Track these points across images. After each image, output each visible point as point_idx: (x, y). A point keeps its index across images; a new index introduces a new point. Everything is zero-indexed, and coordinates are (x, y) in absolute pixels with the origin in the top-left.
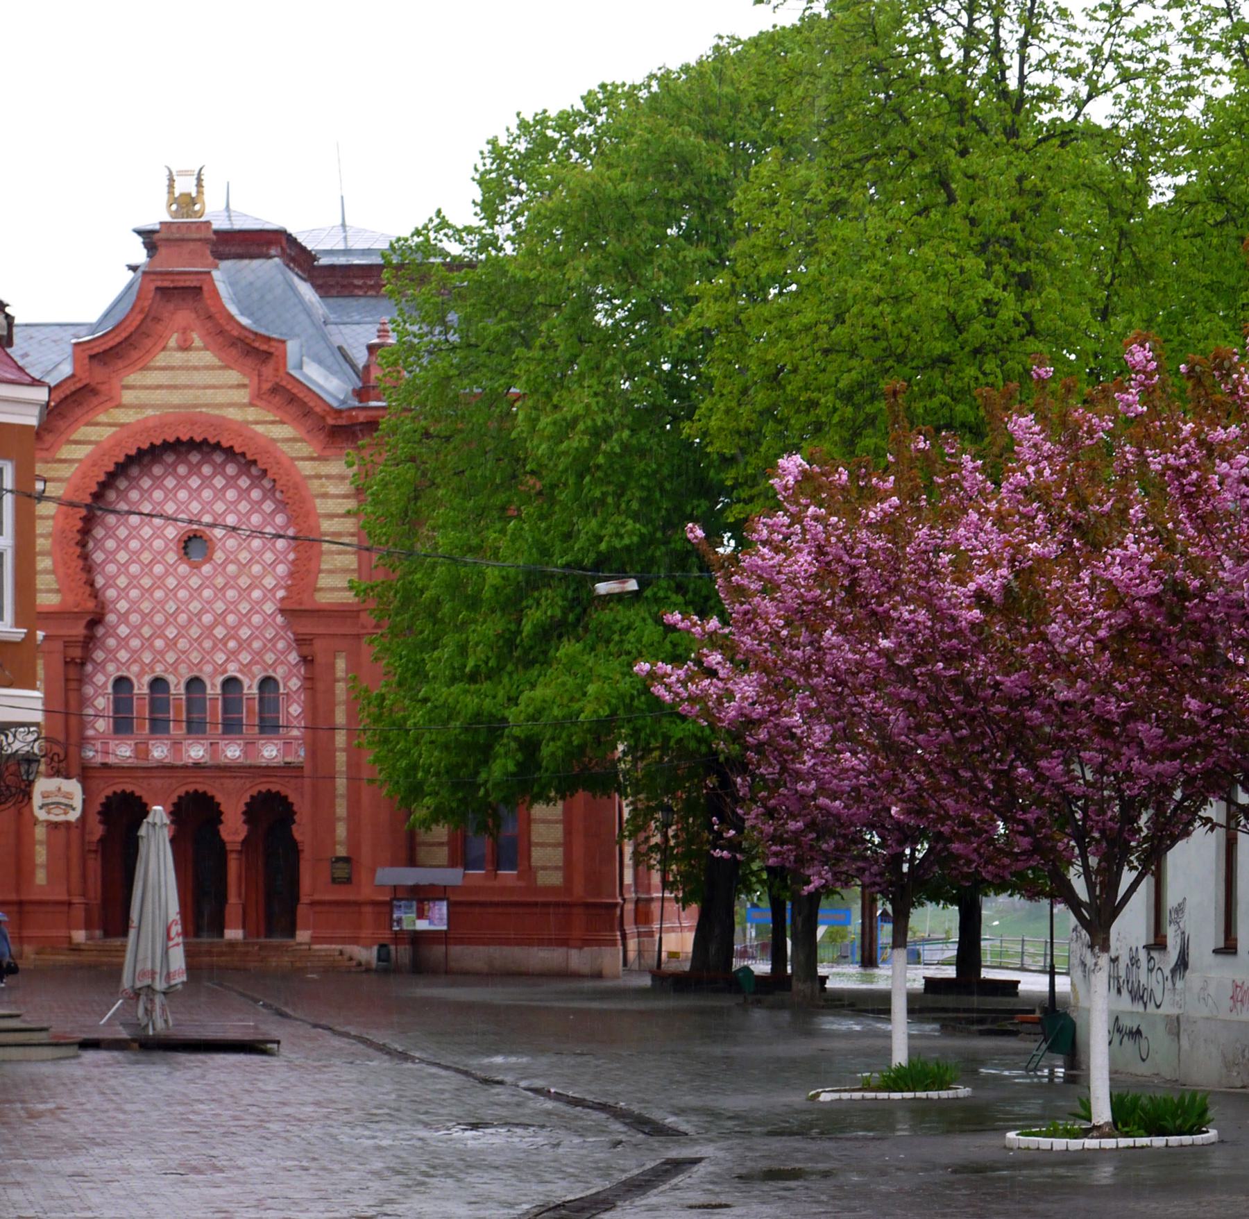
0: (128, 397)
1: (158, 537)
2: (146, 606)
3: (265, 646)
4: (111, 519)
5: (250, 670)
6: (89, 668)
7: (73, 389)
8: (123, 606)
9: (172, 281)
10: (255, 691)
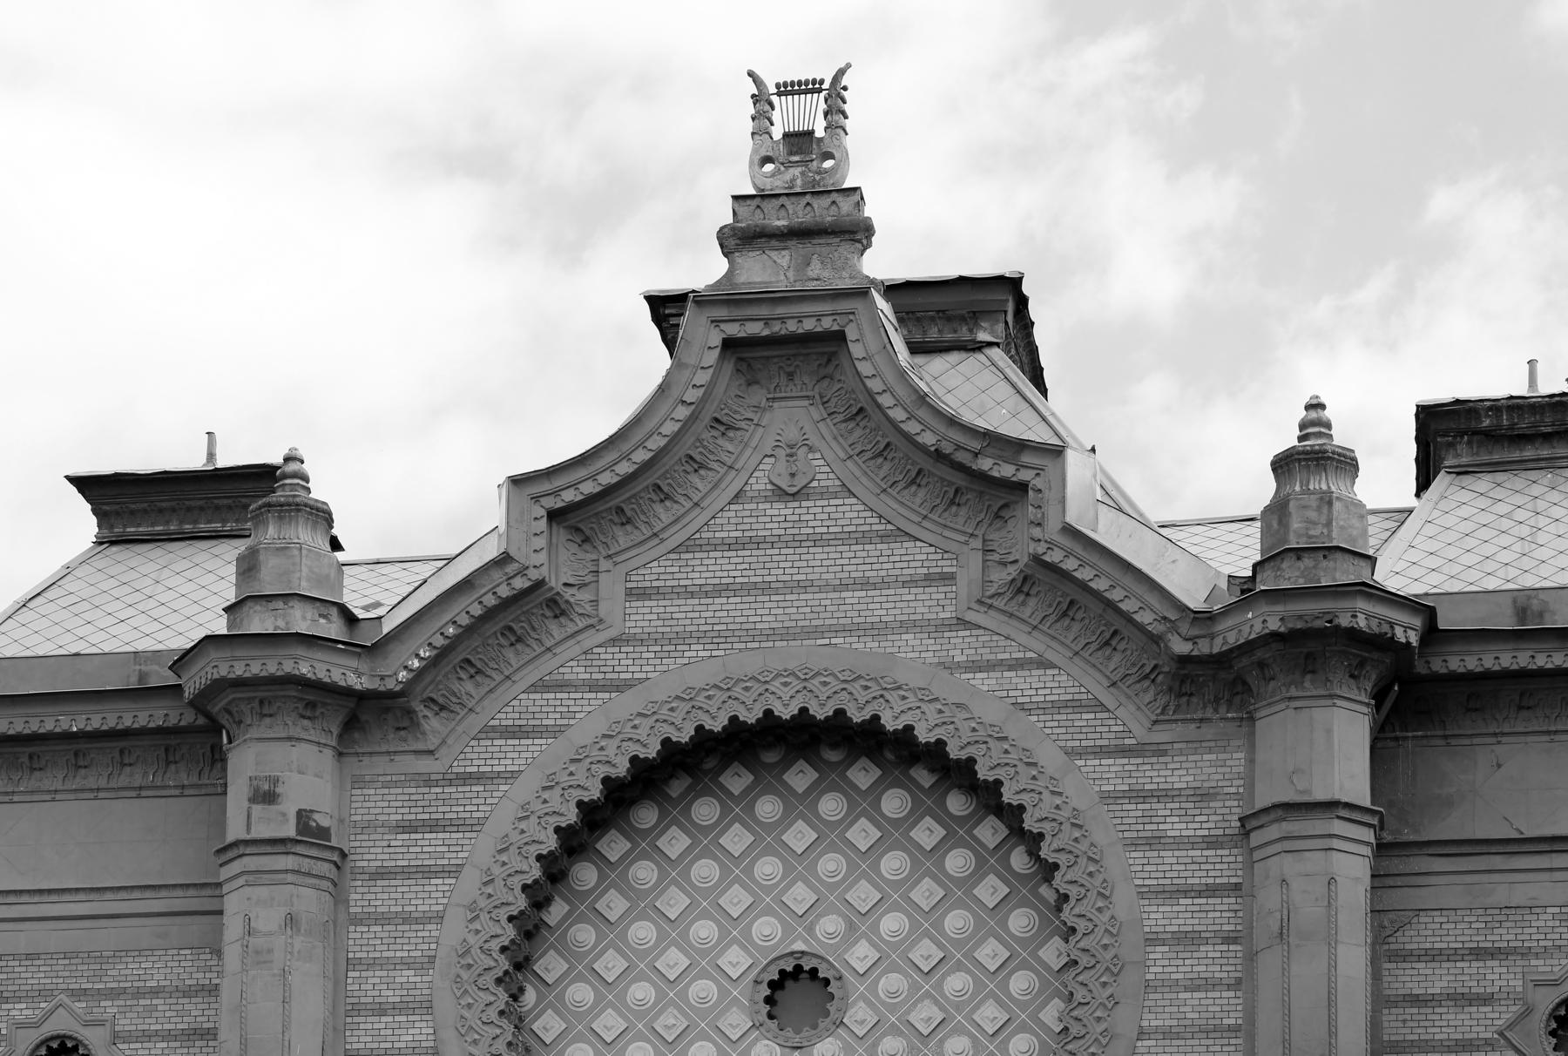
0: (643, 616)
1: (704, 974)
7: (504, 592)
9: (767, 321)
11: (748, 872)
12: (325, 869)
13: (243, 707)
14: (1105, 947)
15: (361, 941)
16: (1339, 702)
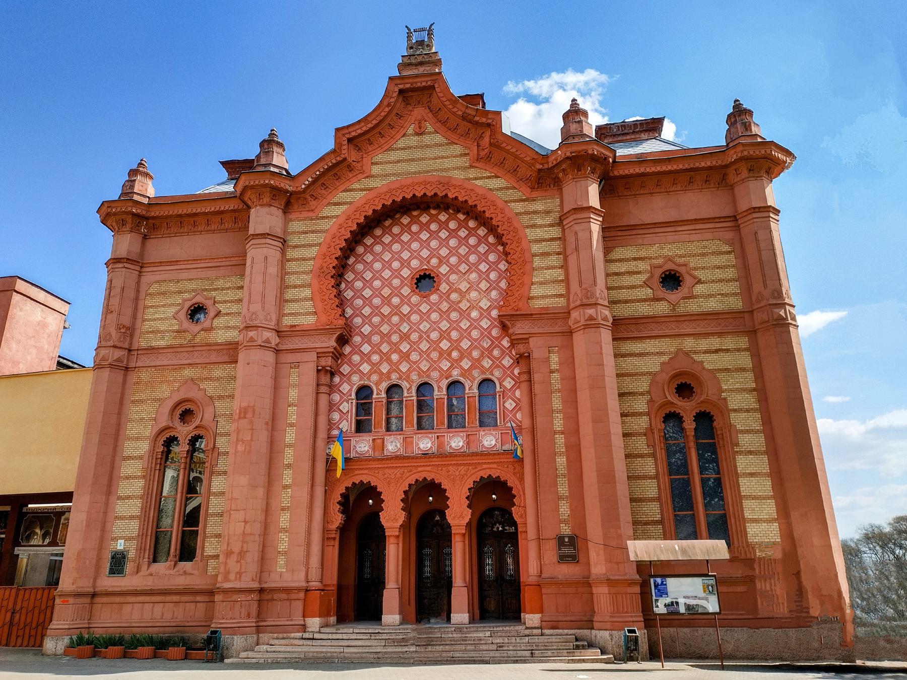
0: (375, 170)
2: (385, 329)
4: (360, 267)
5: (470, 374)
6: (337, 379)
7: (334, 161)
8: (366, 329)
10: (476, 391)
11: (410, 246)
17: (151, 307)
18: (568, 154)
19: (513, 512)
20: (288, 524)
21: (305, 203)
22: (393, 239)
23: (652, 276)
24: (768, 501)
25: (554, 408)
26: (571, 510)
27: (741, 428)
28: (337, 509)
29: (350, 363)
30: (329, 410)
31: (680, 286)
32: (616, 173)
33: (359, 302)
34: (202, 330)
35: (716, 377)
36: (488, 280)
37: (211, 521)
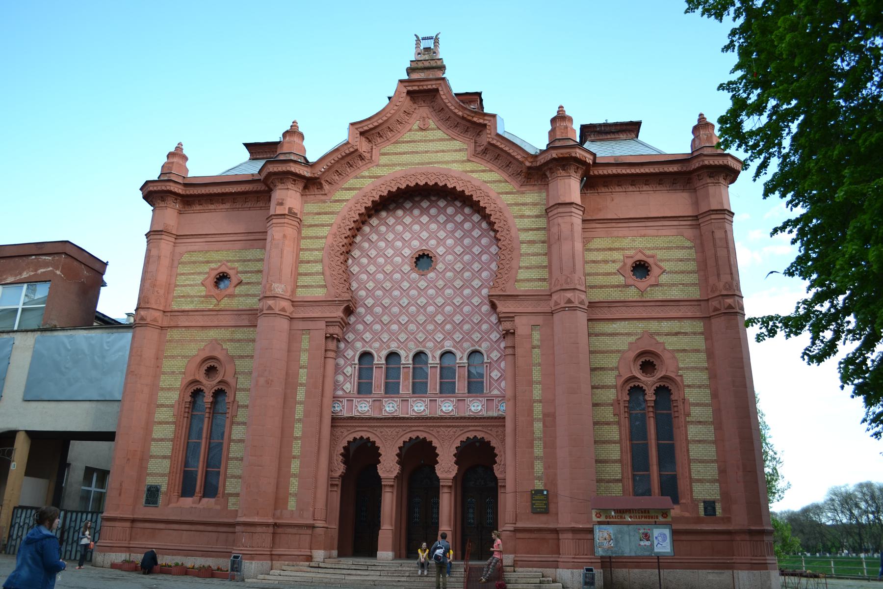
0: (383, 160)
1: (398, 256)
2: (387, 302)
3: (473, 328)
6: (342, 345)
7: (347, 152)
8: (370, 302)
9: (418, 86)
10: (465, 361)
12: (296, 223)
13: (276, 181)
14: (509, 244)
15: (304, 244)
16: (572, 178)
17: (183, 274)
18: (554, 156)
19: (495, 468)
20: (298, 471)
21: (320, 186)
22: (397, 221)
23: (625, 264)
24: (712, 464)
25: (534, 380)
26: (545, 469)
27: (693, 402)
28: (340, 460)
29: (355, 331)
30: (335, 373)
31: (648, 275)
32: (596, 173)
33: (364, 277)
34: (226, 296)
35: (674, 357)
36: (480, 261)
37: (231, 464)
